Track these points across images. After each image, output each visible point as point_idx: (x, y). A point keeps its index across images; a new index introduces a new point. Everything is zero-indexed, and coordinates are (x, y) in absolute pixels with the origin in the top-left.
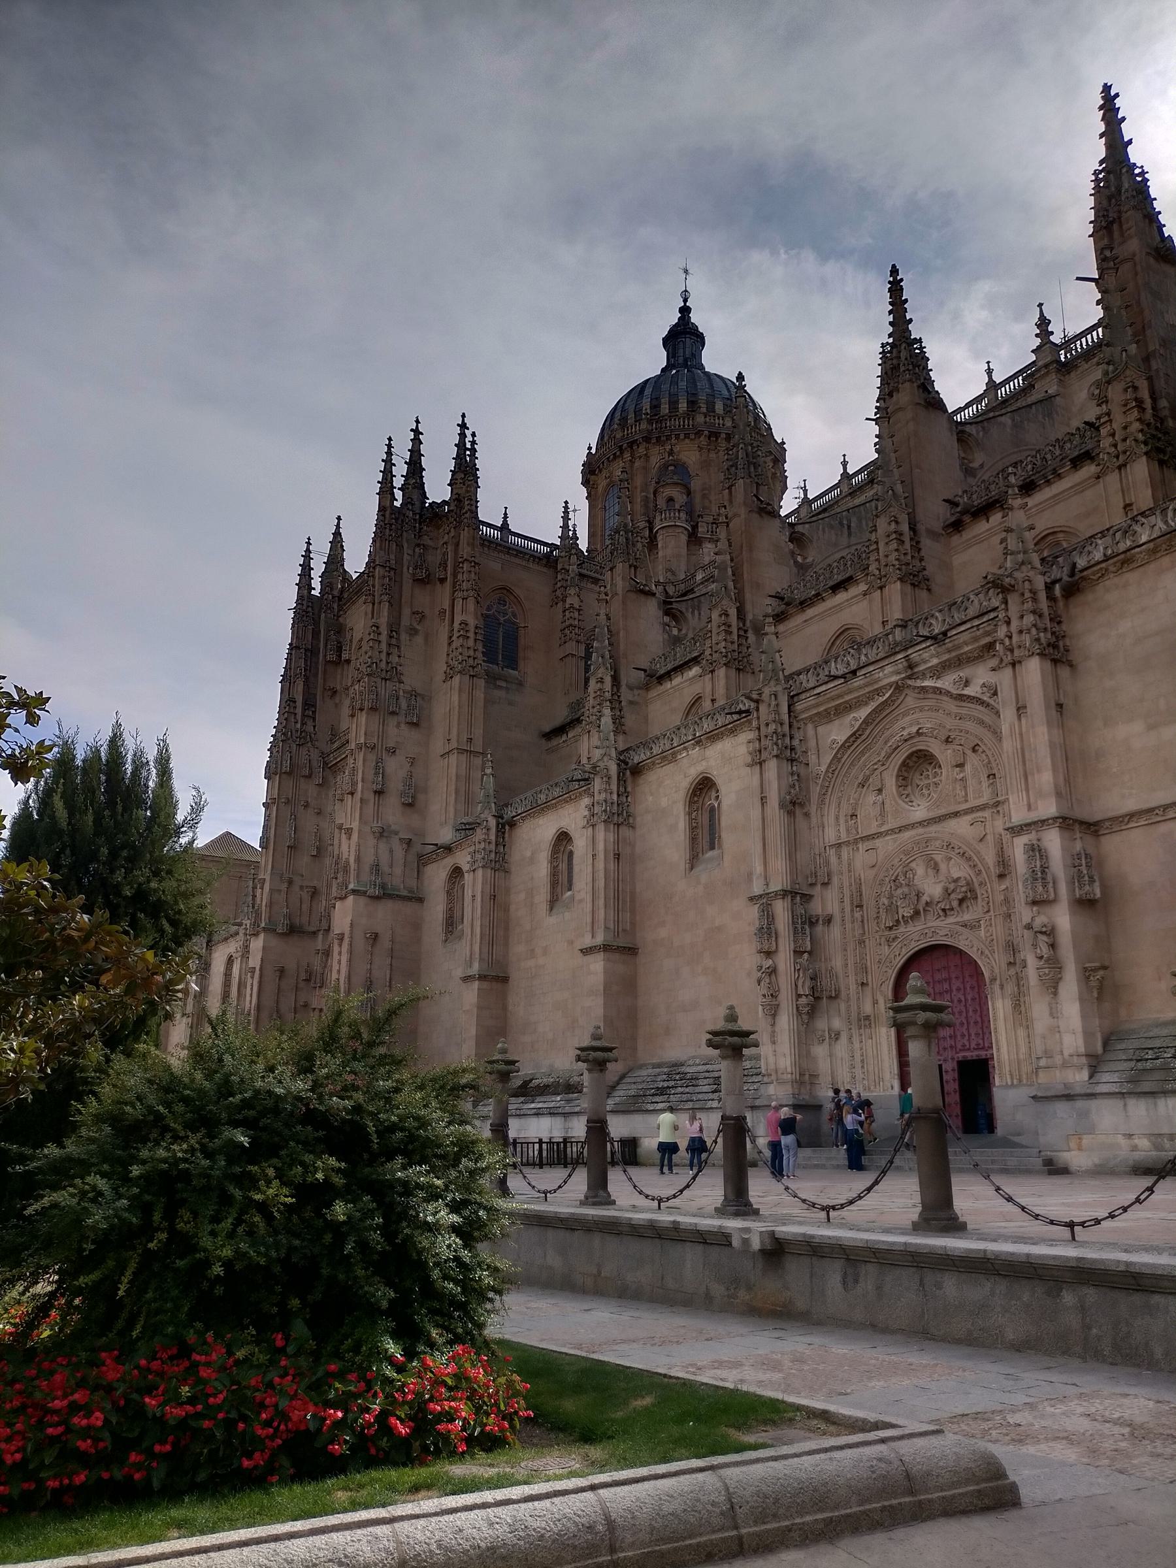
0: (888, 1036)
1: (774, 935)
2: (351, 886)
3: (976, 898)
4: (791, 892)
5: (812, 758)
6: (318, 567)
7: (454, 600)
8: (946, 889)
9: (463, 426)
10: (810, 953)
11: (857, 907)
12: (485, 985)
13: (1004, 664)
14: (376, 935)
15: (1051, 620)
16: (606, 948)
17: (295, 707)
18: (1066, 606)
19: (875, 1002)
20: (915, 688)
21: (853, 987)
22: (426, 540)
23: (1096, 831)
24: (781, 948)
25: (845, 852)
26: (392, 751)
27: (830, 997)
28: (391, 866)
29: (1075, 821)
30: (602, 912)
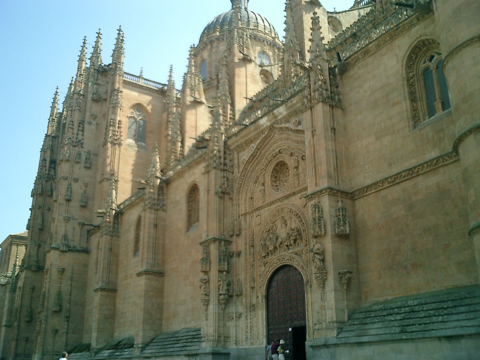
0: (263, 315)
1: (208, 263)
2: (52, 246)
3: (302, 238)
4: (218, 239)
5: (236, 170)
6: (61, 98)
7: (109, 108)
8: (288, 234)
9: (120, 30)
10: (228, 272)
11: (252, 246)
12: (105, 293)
13: (307, 109)
14: (64, 269)
15: (331, 86)
16: (146, 273)
17: (46, 163)
18: (341, 79)
19: (258, 297)
20: (278, 129)
21: (249, 289)
22: (100, 82)
23: (353, 197)
24: (212, 269)
25: (248, 217)
26: (76, 180)
27: (237, 295)
28: (73, 236)
29: (338, 191)
30: (146, 254)
